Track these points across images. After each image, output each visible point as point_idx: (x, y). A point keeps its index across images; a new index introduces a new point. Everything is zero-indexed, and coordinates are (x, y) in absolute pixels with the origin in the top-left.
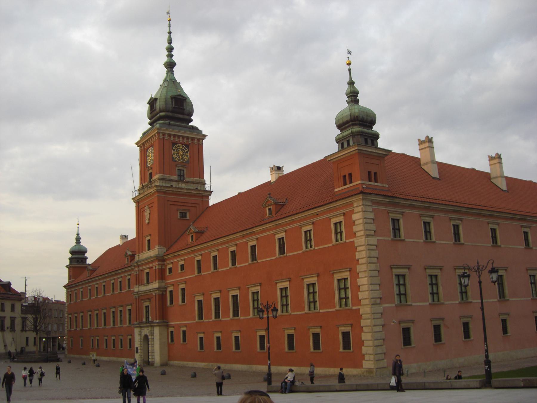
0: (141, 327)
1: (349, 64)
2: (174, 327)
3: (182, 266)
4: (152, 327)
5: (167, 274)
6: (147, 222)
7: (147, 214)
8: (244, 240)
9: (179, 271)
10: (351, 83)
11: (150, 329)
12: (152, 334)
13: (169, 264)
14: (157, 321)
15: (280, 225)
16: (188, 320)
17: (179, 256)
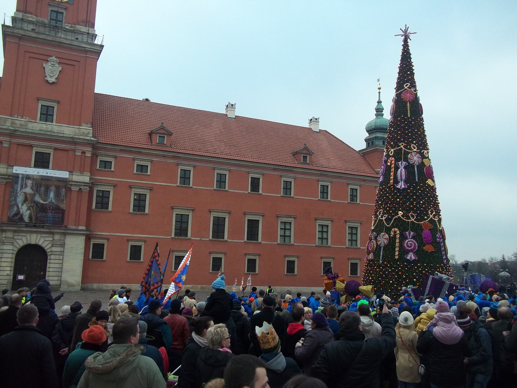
0: (15, 231)
1: (379, 89)
2: (108, 239)
3: (142, 168)
4: (65, 234)
5: (98, 168)
6: (52, 80)
7: (52, 70)
8: (279, 173)
9: (135, 172)
10: (379, 102)
11: (57, 237)
12: (63, 245)
13: (109, 156)
14: (80, 228)
15: (326, 176)
16: (153, 234)
17: (140, 153)
